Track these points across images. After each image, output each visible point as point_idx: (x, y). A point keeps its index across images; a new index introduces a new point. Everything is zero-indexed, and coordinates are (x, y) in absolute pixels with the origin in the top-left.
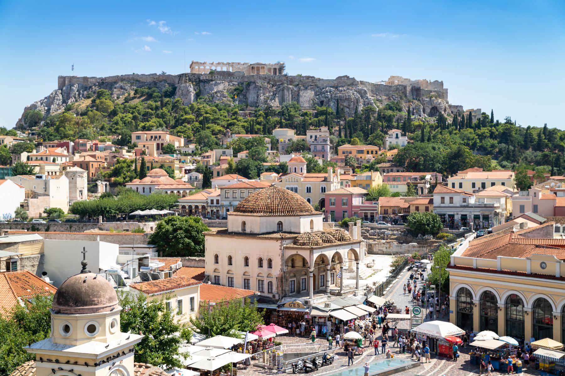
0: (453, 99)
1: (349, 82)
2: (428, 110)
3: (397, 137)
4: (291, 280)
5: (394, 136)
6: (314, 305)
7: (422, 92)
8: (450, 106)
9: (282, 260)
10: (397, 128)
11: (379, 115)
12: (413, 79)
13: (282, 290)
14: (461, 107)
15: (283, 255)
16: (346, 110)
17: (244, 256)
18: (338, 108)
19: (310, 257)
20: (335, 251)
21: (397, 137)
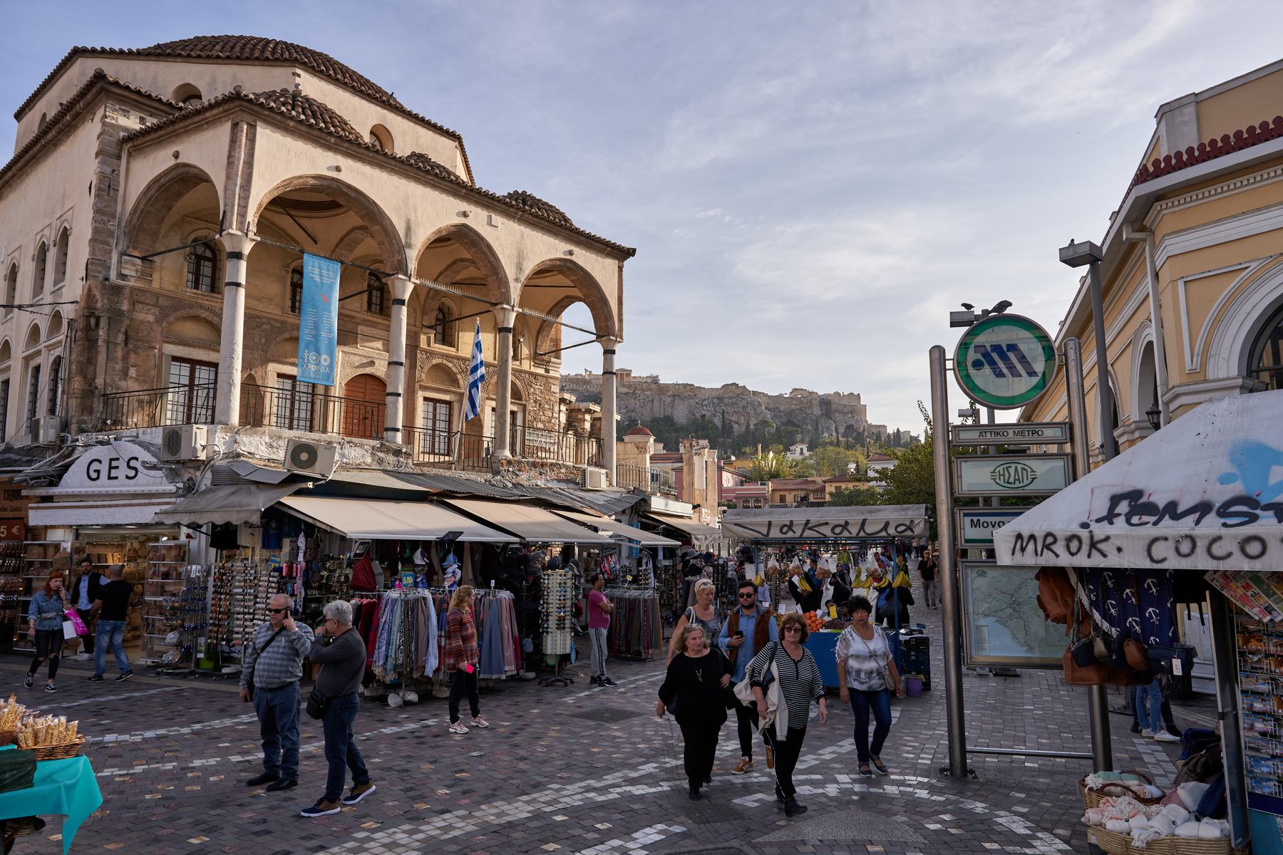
0: (873, 418)
1: (738, 391)
2: (842, 430)
3: (802, 453)
4: (171, 349)
5: (798, 451)
6: (220, 462)
7: (834, 407)
8: (871, 426)
9: (103, 211)
10: (802, 442)
11: (778, 429)
12: (820, 393)
13: (89, 392)
14: (884, 427)
15: (107, 188)
16: (736, 426)
17: (8, 264)
18: (723, 422)
19: (231, 162)
20: (462, 220)
21: (802, 453)
